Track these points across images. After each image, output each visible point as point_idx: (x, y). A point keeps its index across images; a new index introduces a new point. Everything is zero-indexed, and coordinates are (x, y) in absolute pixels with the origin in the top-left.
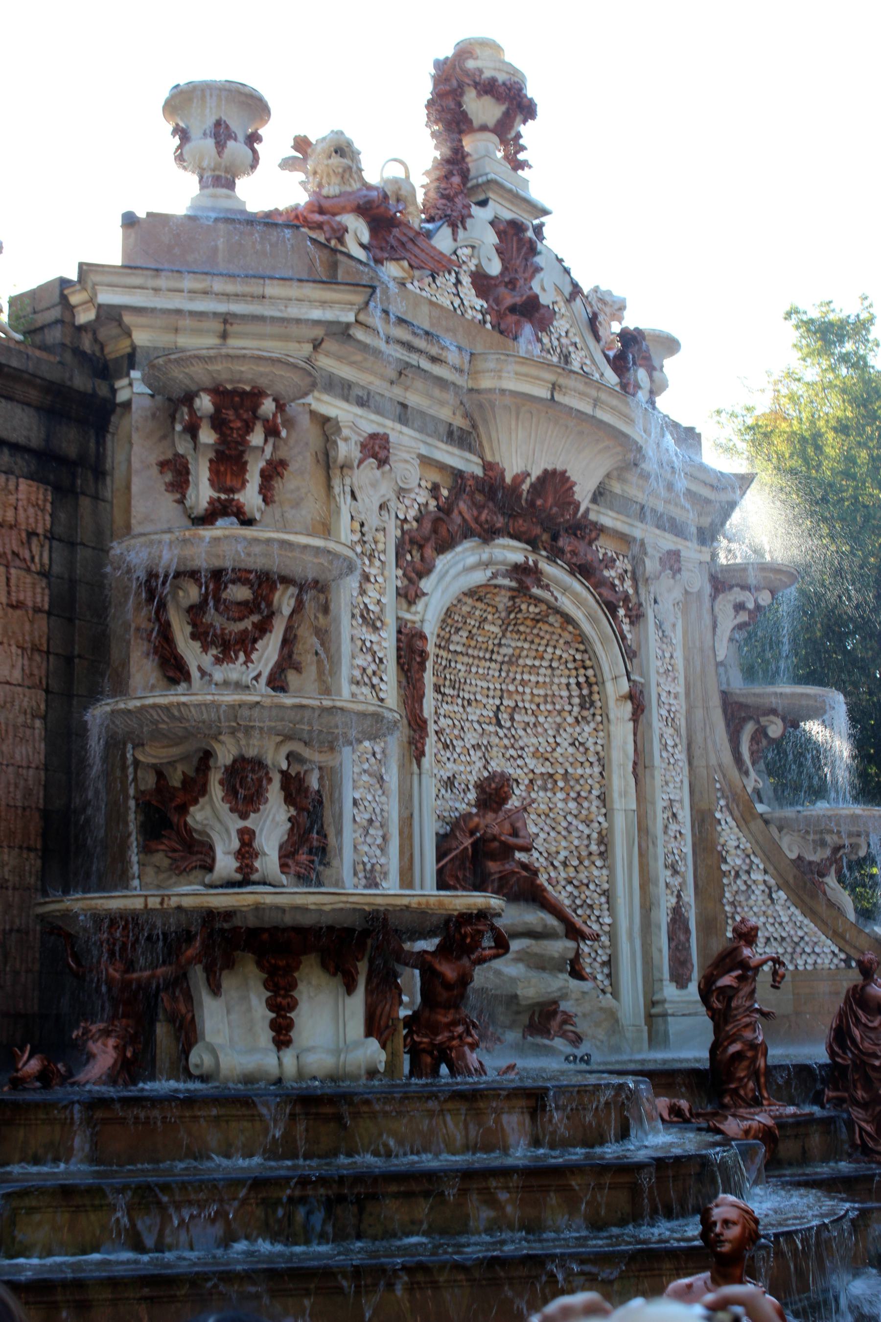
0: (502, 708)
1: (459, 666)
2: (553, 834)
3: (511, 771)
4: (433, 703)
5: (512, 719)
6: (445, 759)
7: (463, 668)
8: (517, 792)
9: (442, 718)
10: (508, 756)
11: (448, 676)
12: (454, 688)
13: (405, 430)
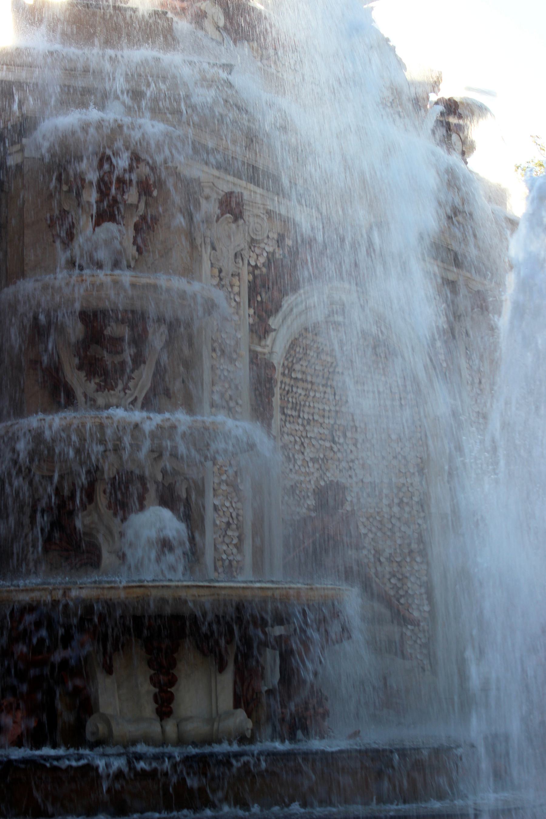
0: (336, 427)
1: (300, 391)
2: (379, 534)
3: (343, 481)
4: (279, 422)
5: (345, 436)
6: (288, 470)
7: (303, 393)
9: (286, 437)
10: (341, 467)
11: (290, 400)
12: (295, 411)
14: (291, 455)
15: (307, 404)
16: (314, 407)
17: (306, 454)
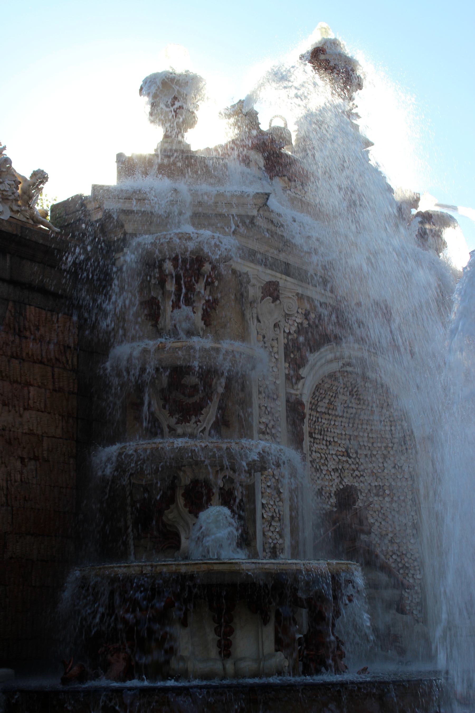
1: (323, 421)
3: (356, 484)
4: (309, 444)
6: (316, 478)
7: (326, 422)
8: (361, 497)
9: (314, 453)
10: (354, 475)
11: (317, 427)
12: (321, 435)
13: (288, 278)
14: (318, 467)
15: (329, 430)
16: (334, 432)
17: (329, 466)
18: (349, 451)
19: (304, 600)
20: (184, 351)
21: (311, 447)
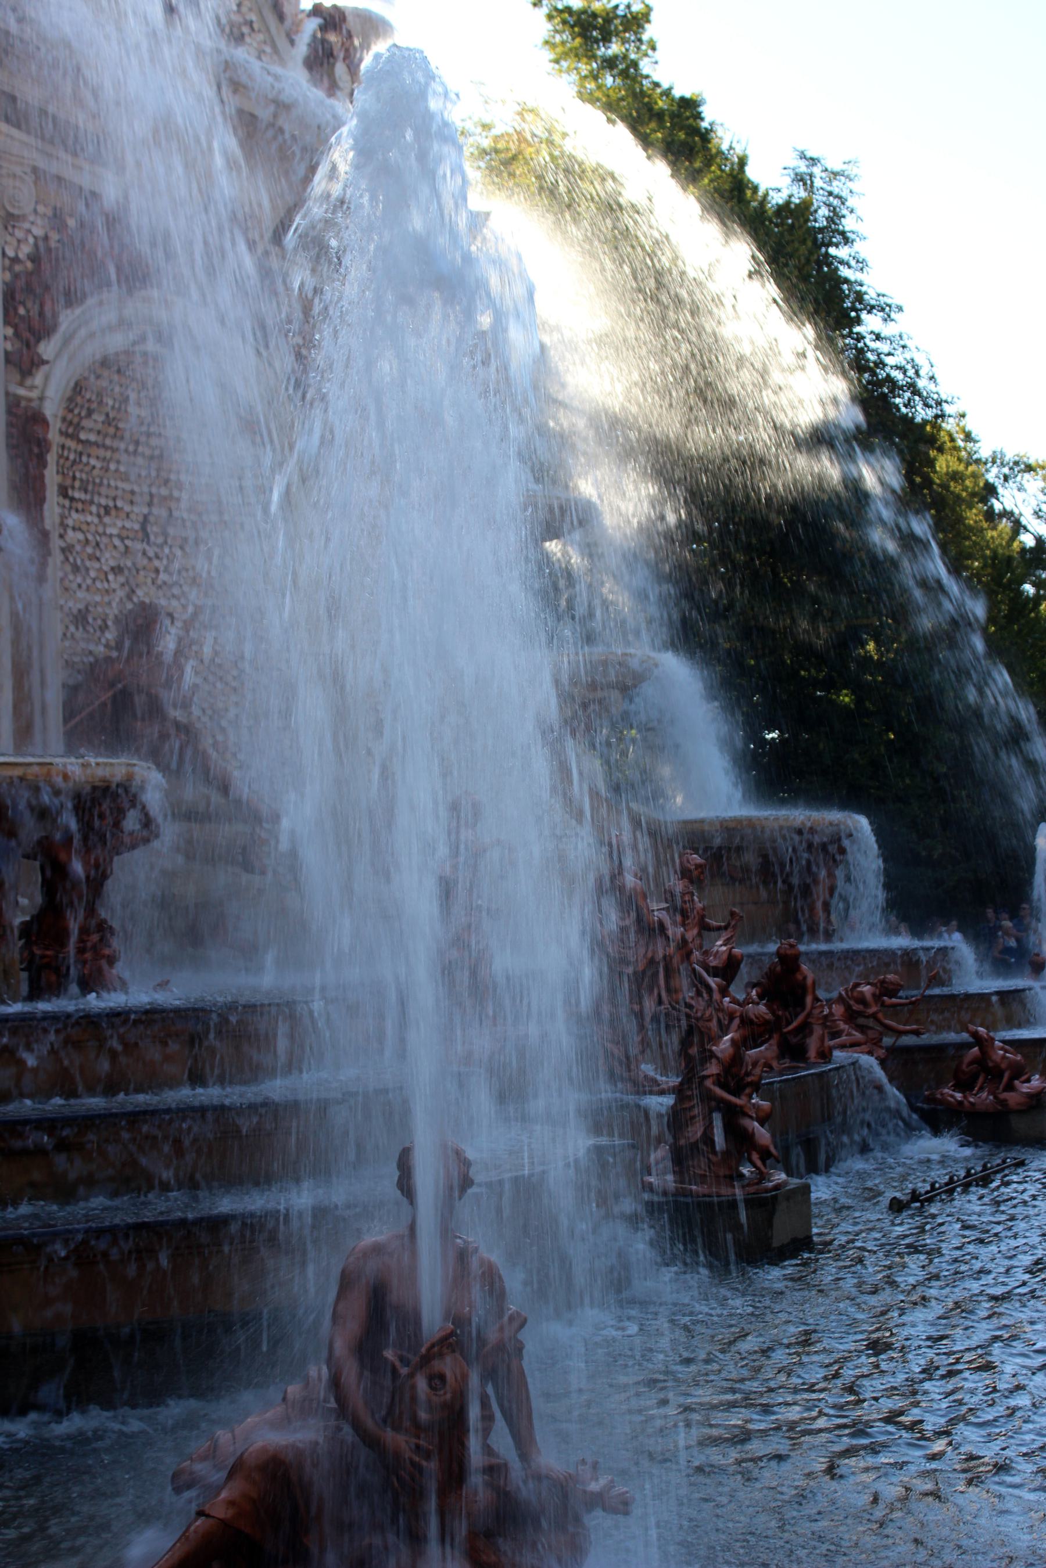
0: (152, 519)
1: (93, 462)
2: (219, 685)
3: (163, 602)
4: (57, 510)
5: (165, 535)
6: (74, 586)
7: (98, 465)
8: (173, 631)
9: (70, 532)
10: (159, 582)
11: (78, 475)
12: (86, 491)
13: (14, 132)
14: (79, 562)
15: (105, 482)
16: (117, 488)
17: (103, 560)
18: (149, 530)
19: (936, 943)
20: (829, 469)
21: (63, 517)
